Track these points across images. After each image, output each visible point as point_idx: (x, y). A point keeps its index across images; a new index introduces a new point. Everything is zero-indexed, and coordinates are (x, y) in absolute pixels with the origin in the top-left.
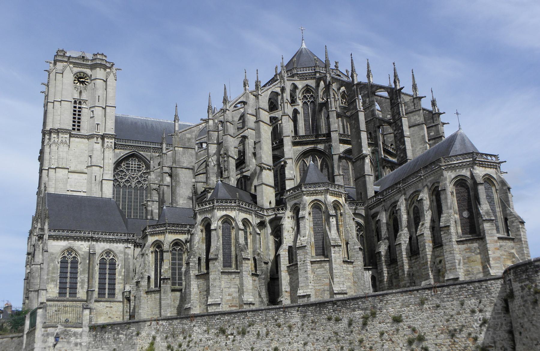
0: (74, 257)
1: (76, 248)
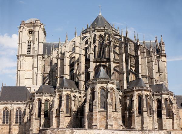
0: (7, 110)
1: (8, 107)
